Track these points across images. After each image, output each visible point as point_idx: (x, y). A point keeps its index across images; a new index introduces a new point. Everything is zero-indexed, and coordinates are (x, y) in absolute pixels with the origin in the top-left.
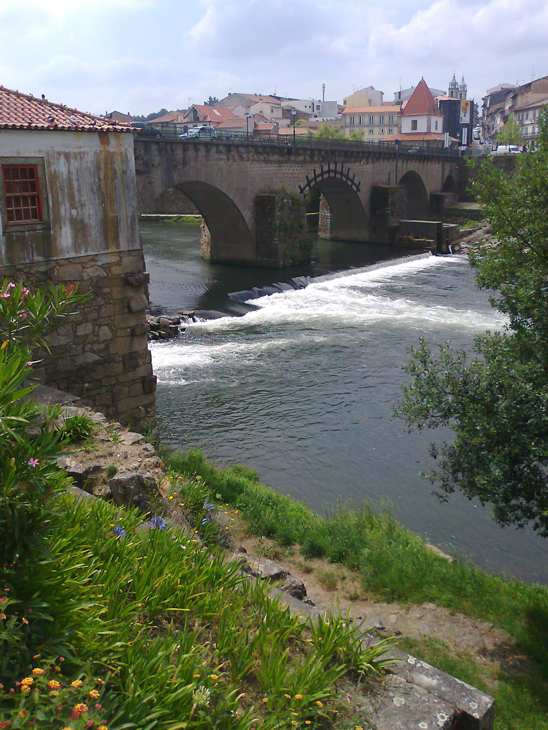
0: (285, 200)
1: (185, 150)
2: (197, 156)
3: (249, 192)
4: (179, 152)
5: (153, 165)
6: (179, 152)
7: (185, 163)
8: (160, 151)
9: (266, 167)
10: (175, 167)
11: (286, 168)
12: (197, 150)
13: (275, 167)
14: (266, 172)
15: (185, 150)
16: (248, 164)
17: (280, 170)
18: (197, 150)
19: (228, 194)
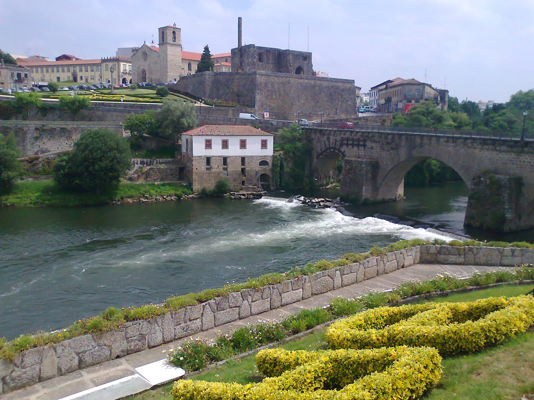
0: (482, 179)
1: (422, 139)
2: (430, 143)
3: (474, 170)
4: (418, 140)
5: (401, 146)
6: (418, 140)
7: (421, 145)
8: (407, 139)
9: (498, 154)
10: (414, 148)
11: (527, 157)
12: (430, 140)
13: (511, 155)
14: (498, 158)
15: (422, 139)
16: (477, 151)
17: (518, 158)
18: (430, 140)
19: (453, 168)
